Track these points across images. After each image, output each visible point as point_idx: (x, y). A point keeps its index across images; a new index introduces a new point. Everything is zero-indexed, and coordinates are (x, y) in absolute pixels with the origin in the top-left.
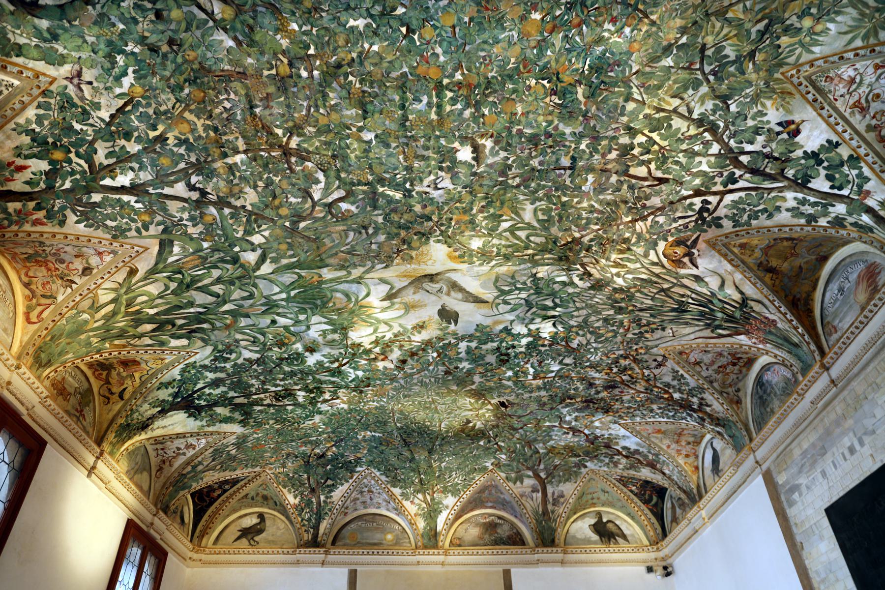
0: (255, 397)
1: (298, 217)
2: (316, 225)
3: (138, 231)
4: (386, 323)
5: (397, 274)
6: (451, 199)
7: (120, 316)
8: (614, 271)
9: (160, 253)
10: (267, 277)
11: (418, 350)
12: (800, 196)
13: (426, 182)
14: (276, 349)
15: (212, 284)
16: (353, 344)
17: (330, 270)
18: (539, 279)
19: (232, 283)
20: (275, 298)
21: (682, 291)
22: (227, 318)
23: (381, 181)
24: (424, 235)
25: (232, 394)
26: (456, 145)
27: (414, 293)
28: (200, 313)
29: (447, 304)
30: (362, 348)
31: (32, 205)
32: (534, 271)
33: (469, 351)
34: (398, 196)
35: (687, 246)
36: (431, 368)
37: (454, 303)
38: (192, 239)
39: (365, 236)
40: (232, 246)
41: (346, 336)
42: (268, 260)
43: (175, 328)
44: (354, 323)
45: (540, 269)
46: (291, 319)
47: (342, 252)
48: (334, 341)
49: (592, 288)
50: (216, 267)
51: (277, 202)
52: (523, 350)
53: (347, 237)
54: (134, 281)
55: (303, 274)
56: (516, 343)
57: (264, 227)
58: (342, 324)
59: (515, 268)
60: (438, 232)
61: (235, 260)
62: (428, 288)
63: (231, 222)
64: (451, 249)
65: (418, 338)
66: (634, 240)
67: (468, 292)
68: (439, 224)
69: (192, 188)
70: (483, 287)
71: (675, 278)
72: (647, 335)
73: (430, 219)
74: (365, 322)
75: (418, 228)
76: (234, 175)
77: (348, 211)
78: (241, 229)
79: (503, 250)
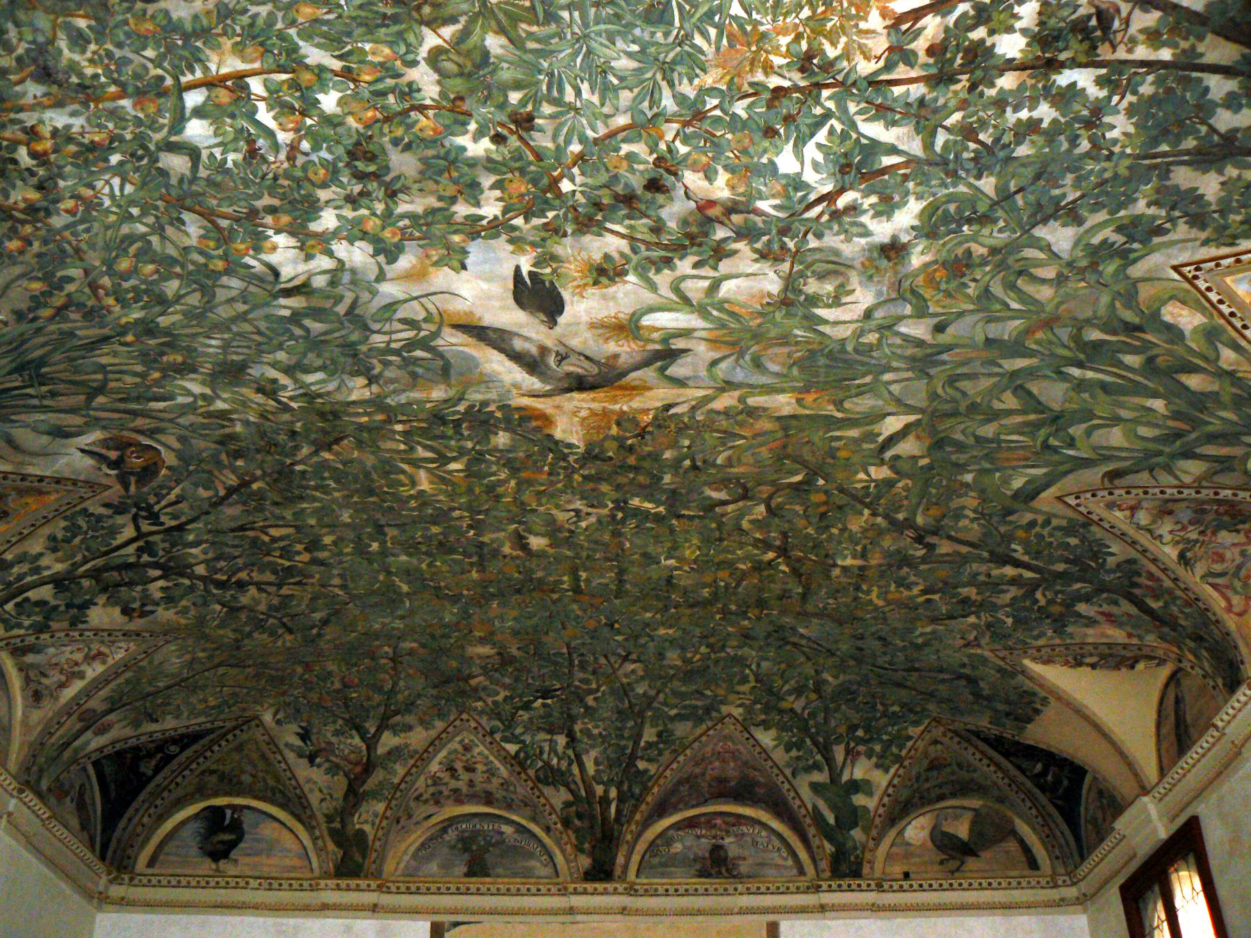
0: (1166, 54)
1: (798, 489)
2: (775, 476)
3: (1047, 522)
4: (686, 300)
5: (648, 394)
6: (552, 496)
7: (1210, 428)
8: (220, 405)
9: (1047, 486)
10: (902, 409)
11: (613, 208)
12: (46, 573)
13: (593, 519)
14: (979, 250)
15: (1010, 412)
16: (778, 259)
17: (778, 409)
18: (357, 373)
19: (973, 408)
20: (910, 374)
21: (63, 401)
22: (1038, 342)
23: (658, 518)
24: (596, 457)
25: (1218, 86)
26: (550, 551)
27: (616, 356)
28: (1080, 365)
29: (544, 329)
30: (758, 245)
31: (1137, 591)
32: (375, 388)
33: (472, 191)
34: (635, 502)
35: (132, 474)
36: (576, 148)
37: (527, 327)
38: (983, 491)
39: (699, 457)
40: (930, 467)
41: (790, 283)
42: (881, 439)
43: (1155, 352)
44: (761, 314)
45: (367, 394)
46: (898, 334)
47: (744, 437)
48: (821, 277)
49: (242, 367)
50: (979, 440)
51: (823, 509)
52: (323, 195)
53: (729, 459)
54: (1128, 463)
55: (831, 407)
56: (348, 213)
57: (859, 486)
58: (789, 315)
59: (415, 395)
60: (571, 459)
61: (938, 444)
62: (586, 364)
63: (905, 502)
64: (547, 431)
65: (611, 244)
66: (224, 457)
67: (502, 350)
68: (570, 471)
69: (931, 547)
70: (472, 358)
71: (98, 419)
72: (36, 286)
73: (584, 477)
74: (732, 314)
75: (606, 468)
76: (864, 548)
77: (716, 490)
78: (894, 490)
79: (450, 432)
